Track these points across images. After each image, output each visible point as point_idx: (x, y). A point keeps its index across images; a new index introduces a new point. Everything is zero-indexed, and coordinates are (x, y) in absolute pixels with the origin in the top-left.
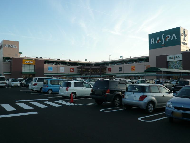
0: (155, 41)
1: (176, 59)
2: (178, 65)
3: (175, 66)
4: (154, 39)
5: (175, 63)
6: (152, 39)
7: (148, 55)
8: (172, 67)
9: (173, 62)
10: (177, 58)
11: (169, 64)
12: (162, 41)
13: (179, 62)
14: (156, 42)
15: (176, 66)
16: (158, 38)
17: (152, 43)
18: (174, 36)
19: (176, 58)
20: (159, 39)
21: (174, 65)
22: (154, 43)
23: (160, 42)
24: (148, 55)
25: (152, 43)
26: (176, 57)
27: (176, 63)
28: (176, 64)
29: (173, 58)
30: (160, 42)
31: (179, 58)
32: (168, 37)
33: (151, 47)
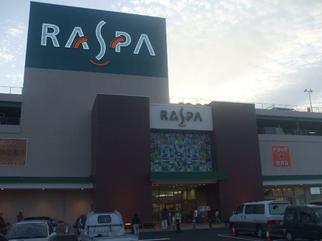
0: (62, 37)
1: (186, 122)
2: (189, 150)
3: (176, 153)
4: (57, 29)
5: (176, 142)
6: (45, 26)
7: (19, 92)
8: (166, 155)
9: (167, 135)
10: (192, 120)
11: (207, 143)
12: (95, 47)
13: (191, 136)
14: (68, 45)
15: (181, 155)
16: (78, 31)
17: (44, 43)
18: (144, 40)
19: (188, 119)
20: (81, 35)
21: (175, 148)
22: (56, 44)
23: (85, 46)
24: (19, 92)
25: (44, 43)
26: (188, 113)
27: (182, 143)
28: (180, 147)
29: (176, 119)
30: (85, 46)
31: (201, 120)
32: (123, 39)
33: (38, 56)
